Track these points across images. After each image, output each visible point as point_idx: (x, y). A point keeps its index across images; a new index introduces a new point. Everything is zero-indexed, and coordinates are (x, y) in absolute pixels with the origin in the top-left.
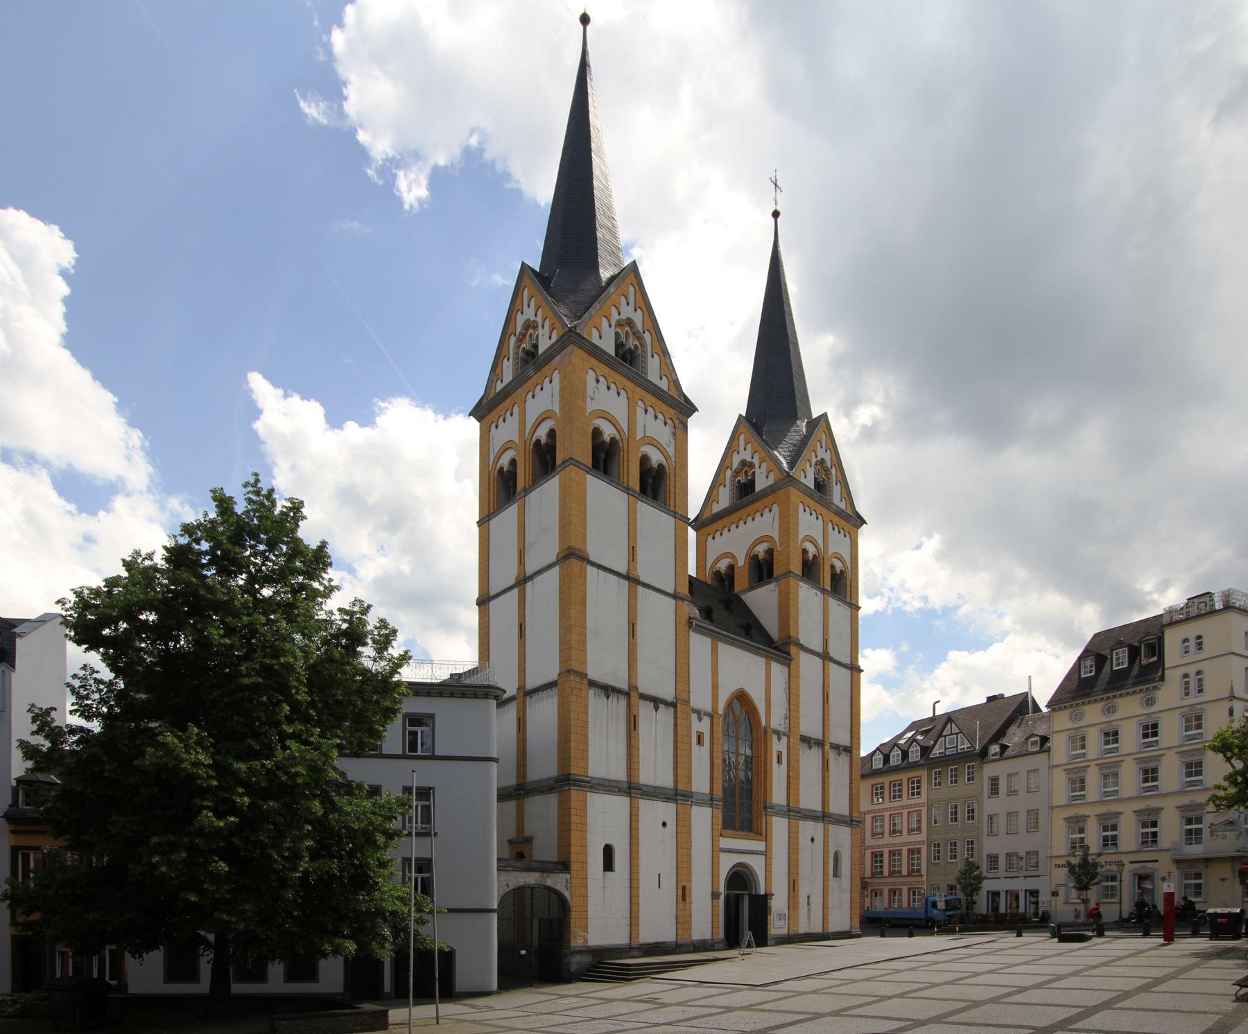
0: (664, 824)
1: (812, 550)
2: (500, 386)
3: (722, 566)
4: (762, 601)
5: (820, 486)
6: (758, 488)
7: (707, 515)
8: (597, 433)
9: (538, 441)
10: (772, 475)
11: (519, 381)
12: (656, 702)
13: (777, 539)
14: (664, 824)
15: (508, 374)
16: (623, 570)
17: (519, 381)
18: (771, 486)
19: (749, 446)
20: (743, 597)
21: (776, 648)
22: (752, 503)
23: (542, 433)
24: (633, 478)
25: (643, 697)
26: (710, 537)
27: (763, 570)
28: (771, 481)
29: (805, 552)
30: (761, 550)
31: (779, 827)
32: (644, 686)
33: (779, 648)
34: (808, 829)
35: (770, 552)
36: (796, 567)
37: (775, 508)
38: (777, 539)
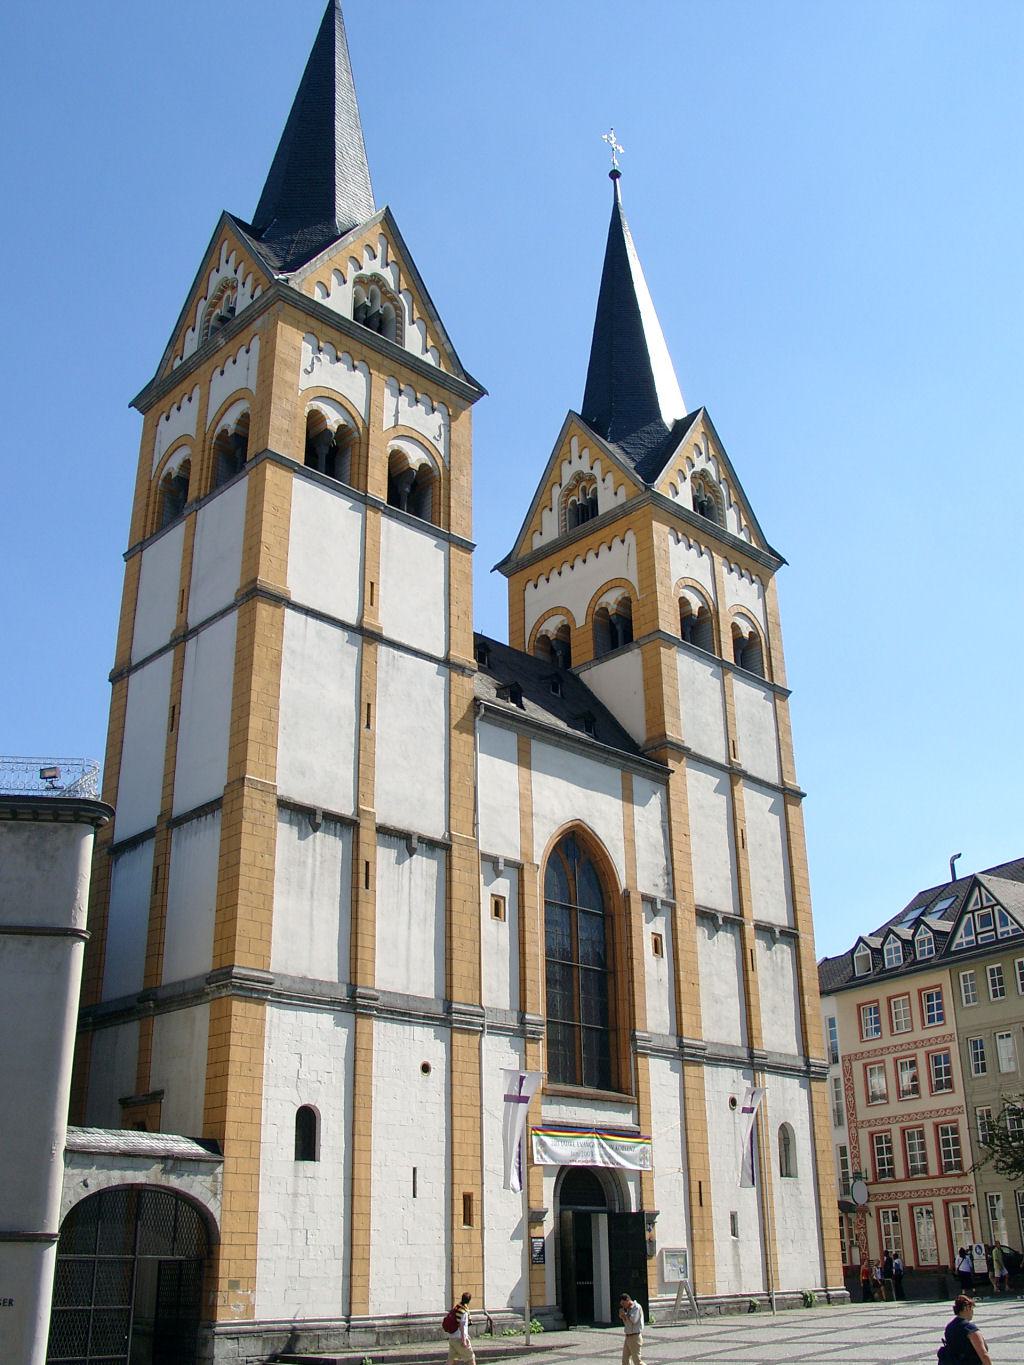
0: (426, 1068)
1: (695, 604)
2: (178, 363)
3: (551, 627)
4: (613, 681)
5: (706, 506)
6: (602, 510)
7: (524, 552)
8: (315, 418)
9: (225, 431)
10: (622, 491)
11: (206, 352)
12: (405, 841)
13: (635, 583)
14: (426, 1068)
15: (191, 343)
16: (352, 620)
17: (206, 352)
18: (622, 505)
19: (586, 453)
20: (585, 677)
21: (641, 754)
22: (593, 531)
23: (230, 421)
24: (378, 485)
25: (383, 831)
26: (530, 585)
27: (617, 630)
28: (622, 498)
29: (684, 603)
30: (611, 600)
31: (659, 1078)
32: (386, 811)
33: (641, 756)
34: (722, 1082)
35: (626, 603)
36: (670, 624)
37: (630, 537)
38: (635, 583)
